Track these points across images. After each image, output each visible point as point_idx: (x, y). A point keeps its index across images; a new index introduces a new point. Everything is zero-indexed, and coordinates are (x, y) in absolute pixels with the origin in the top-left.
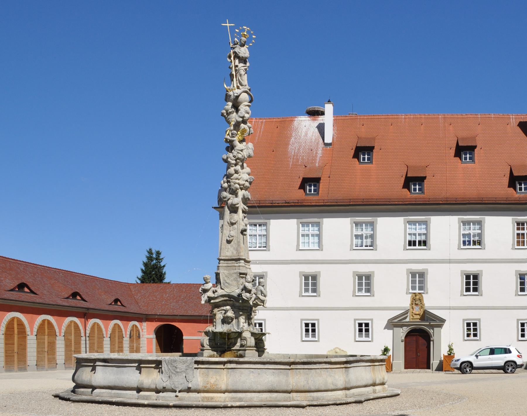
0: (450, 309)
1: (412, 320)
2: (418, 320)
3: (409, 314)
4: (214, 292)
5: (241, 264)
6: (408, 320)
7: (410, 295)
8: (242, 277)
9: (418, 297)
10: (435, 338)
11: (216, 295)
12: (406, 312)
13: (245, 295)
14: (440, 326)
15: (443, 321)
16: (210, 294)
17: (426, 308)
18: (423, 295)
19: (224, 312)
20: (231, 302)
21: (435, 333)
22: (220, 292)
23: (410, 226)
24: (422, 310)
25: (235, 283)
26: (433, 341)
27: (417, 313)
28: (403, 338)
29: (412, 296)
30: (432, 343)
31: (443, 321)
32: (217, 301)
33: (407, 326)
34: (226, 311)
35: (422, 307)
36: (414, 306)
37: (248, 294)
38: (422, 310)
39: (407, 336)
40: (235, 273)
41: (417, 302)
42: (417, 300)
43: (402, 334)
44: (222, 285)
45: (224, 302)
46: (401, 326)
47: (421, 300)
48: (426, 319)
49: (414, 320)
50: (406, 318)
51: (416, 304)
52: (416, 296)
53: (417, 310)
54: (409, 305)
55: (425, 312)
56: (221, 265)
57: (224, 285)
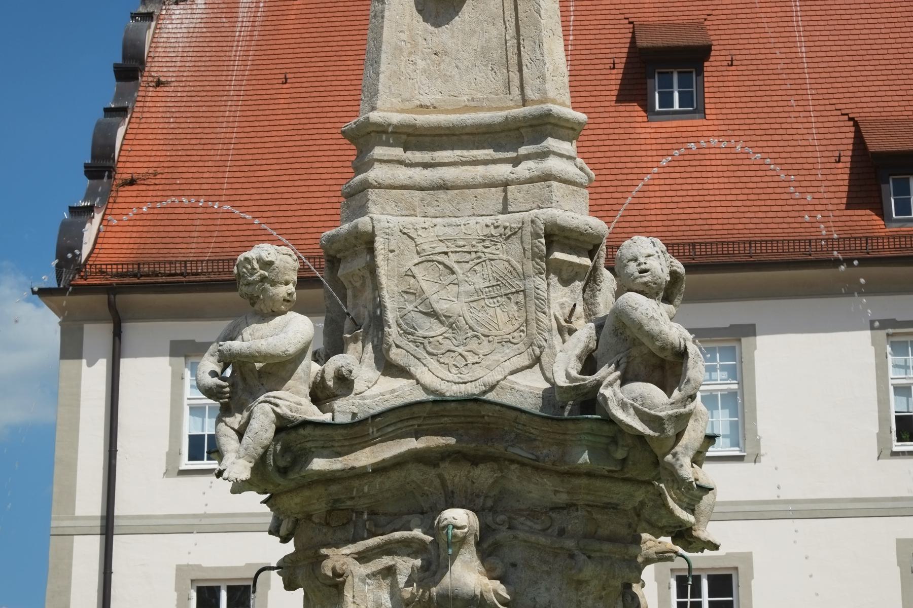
4: (320, 395)
5: (553, 164)
8: (567, 275)
11: (343, 410)
13: (629, 401)
16: (293, 398)
19: (406, 565)
20: (483, 475)
22: (375, 391)
23: (900, 359)
25: (502, 317)
32: (364, 458)
34: (434, 563)
37: (651, 393)
40: (510, 234)
44: (393, 332)
45: (415, 474)
56: (376, 173)
57: (408, 331)
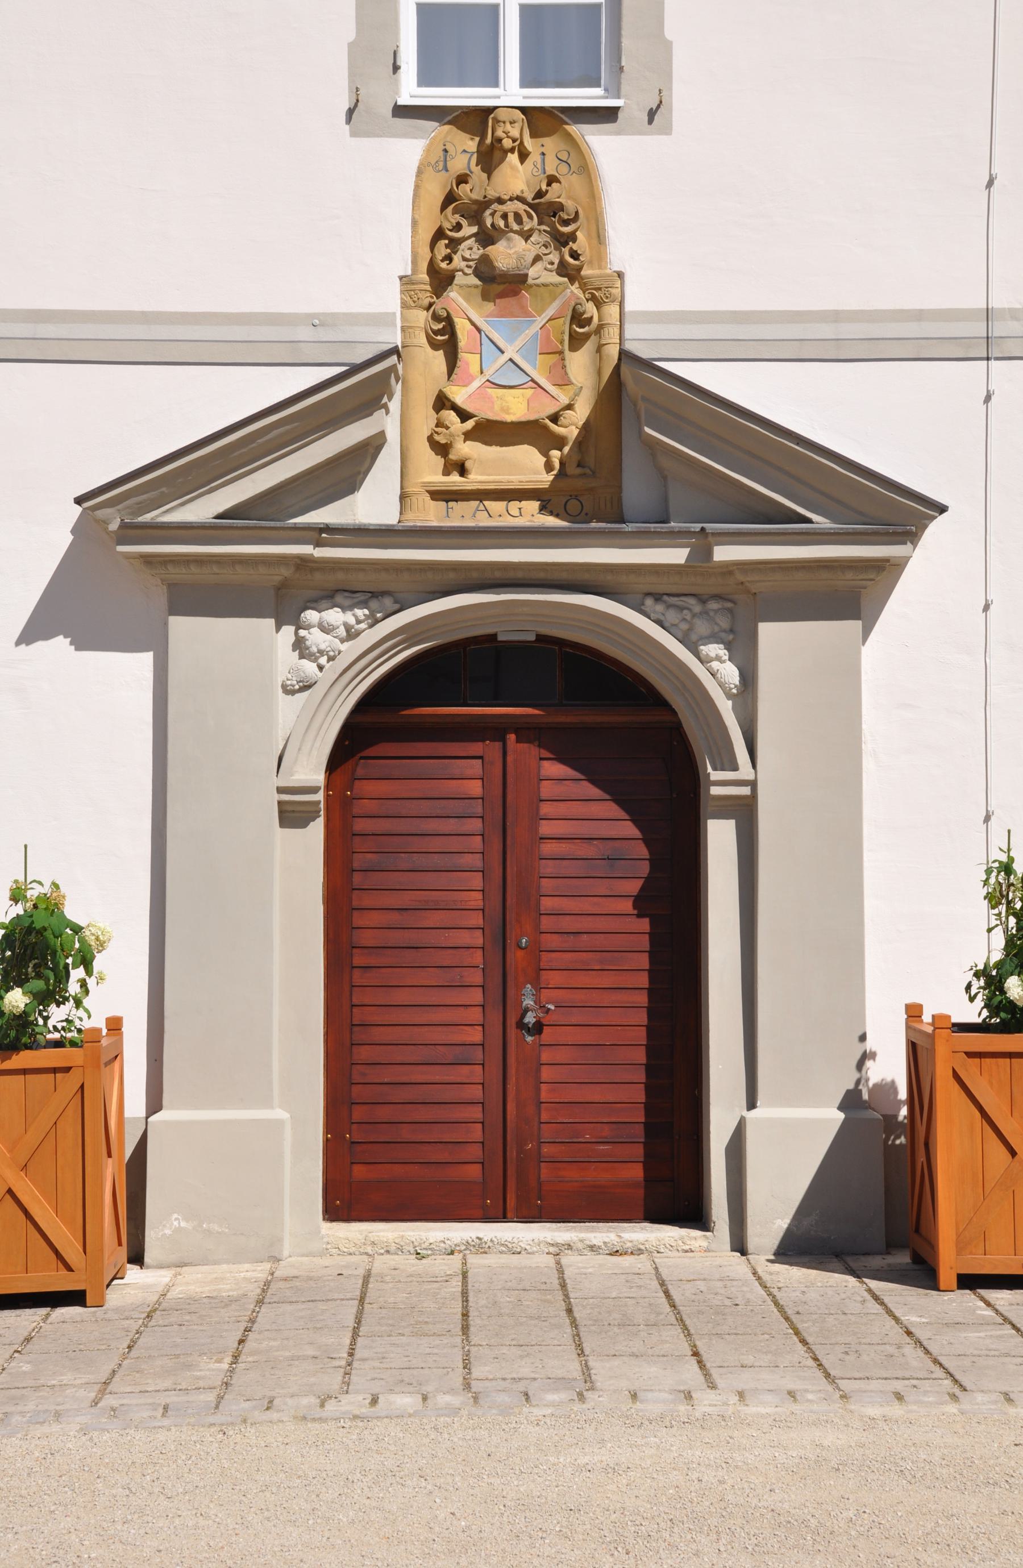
0: (988, 350)
1: (432, 514)
2: (528, 514)
3: (388, 422)
6: (374, 503)
7: (409, 149)
9: (515, 178)
10: (773, 768)
12: (361, 388)
14: (849, 596)
15: (899, 514)
17: (641, 339)
18: (597, 140)
21: (777, 700)
24: (579, 365)
26: (745, 812)
27: (515, 407)
28: (310, 770)
29: (438, 159)
30: (720, 837)
31: (899, 514)
33: (371, 590)
35: (579, 330)
36: (462, 301)
38: (579, 365)
39: (356, 743)
41: (507, 254)
42: (505, 216)
43: (288, 711)
46: (285, 596)
47: (558, 220)
48: (636, 488)
49: (464, 515)
50: (347, 473)
51: (501, 286)
52: (490, 157)
53: (510, 367)
54: (391, 300)
55: (632, 390)
